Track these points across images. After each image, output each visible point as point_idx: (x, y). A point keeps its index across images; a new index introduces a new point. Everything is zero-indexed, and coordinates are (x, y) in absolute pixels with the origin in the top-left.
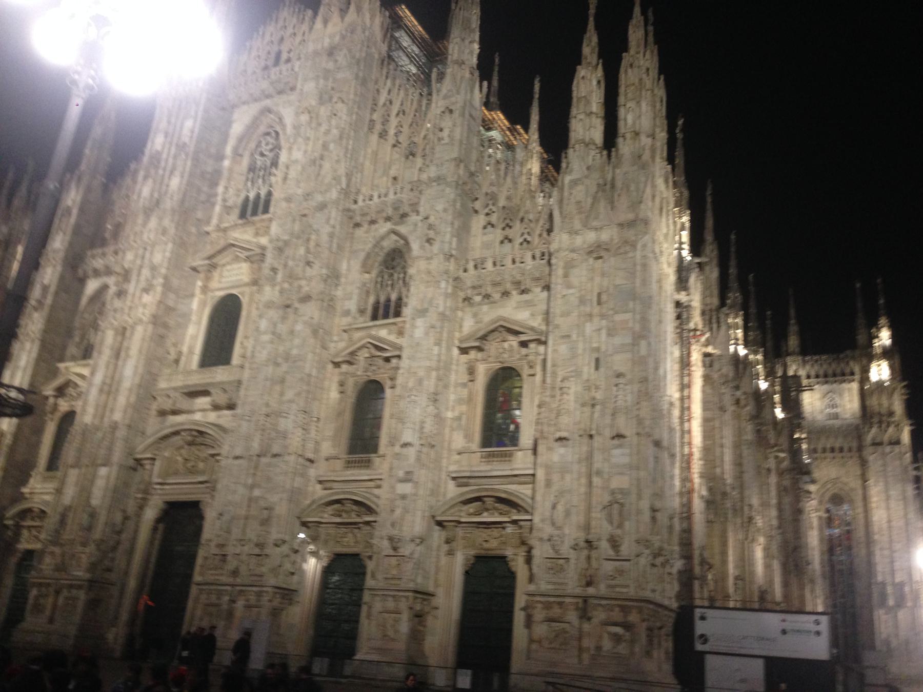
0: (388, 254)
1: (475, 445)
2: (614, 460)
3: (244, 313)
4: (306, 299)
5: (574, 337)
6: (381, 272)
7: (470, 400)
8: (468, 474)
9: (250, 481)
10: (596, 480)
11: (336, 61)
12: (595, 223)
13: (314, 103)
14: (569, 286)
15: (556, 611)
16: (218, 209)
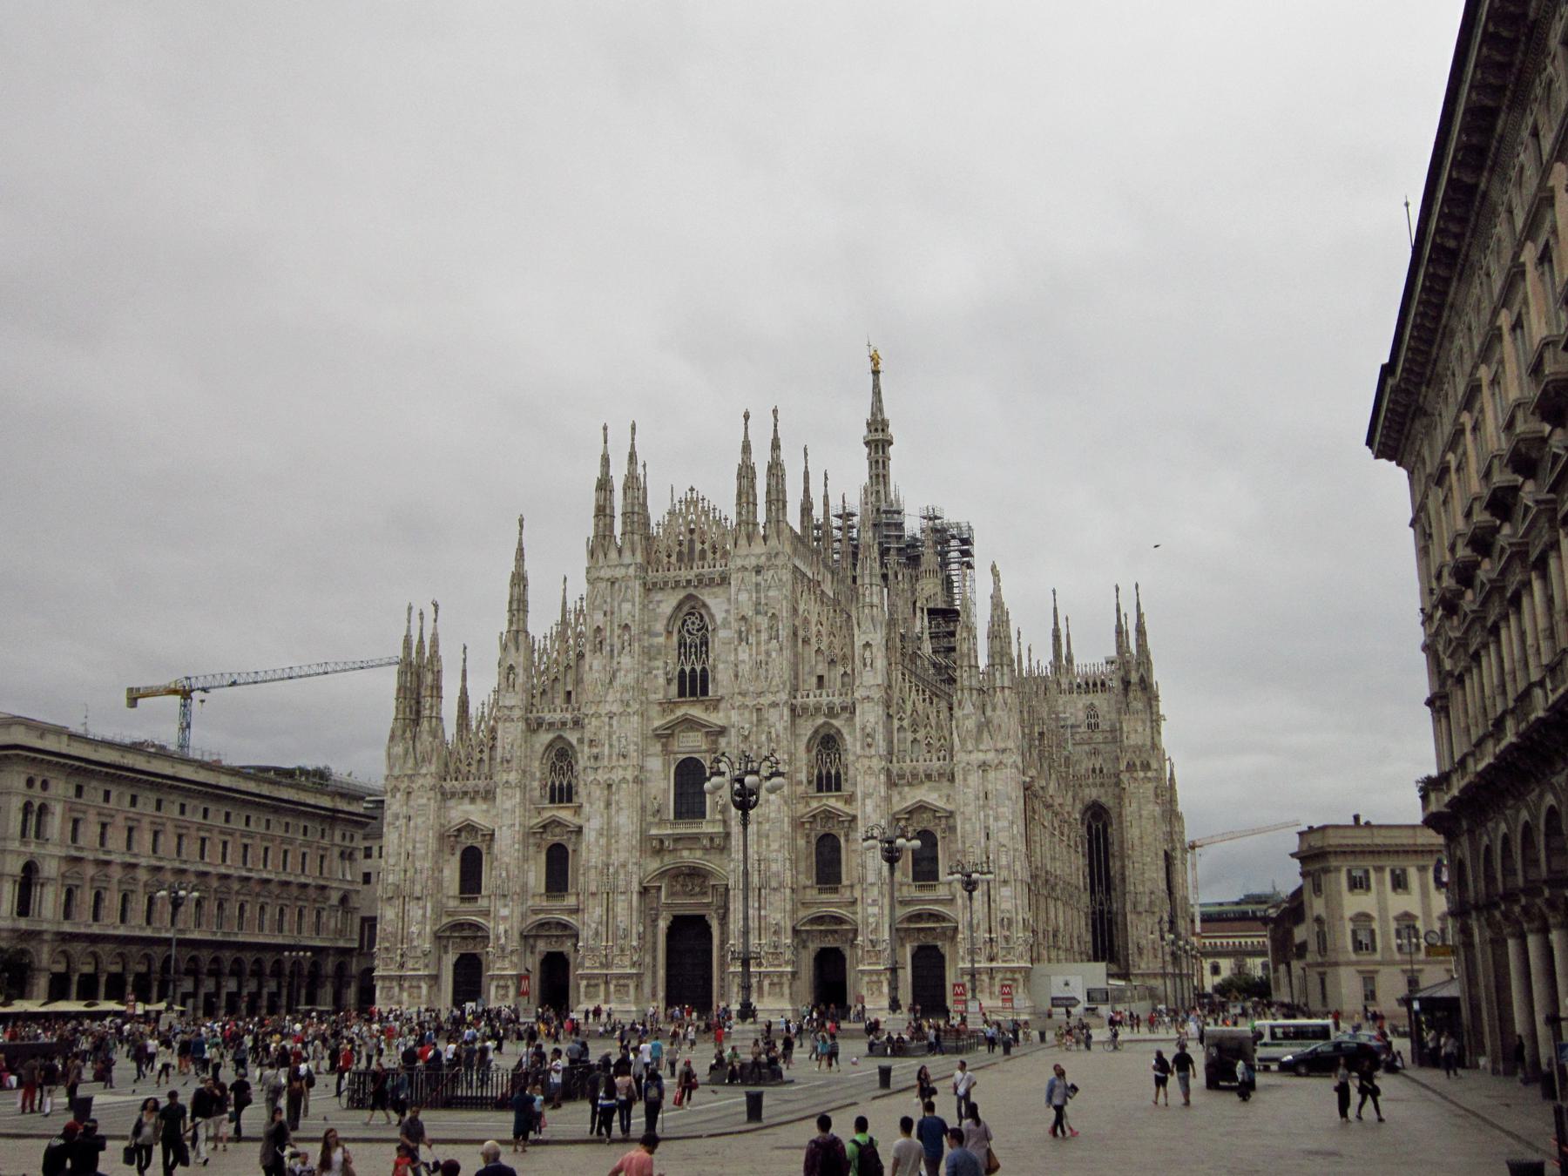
1: (910, 880)
16: (661, 681)
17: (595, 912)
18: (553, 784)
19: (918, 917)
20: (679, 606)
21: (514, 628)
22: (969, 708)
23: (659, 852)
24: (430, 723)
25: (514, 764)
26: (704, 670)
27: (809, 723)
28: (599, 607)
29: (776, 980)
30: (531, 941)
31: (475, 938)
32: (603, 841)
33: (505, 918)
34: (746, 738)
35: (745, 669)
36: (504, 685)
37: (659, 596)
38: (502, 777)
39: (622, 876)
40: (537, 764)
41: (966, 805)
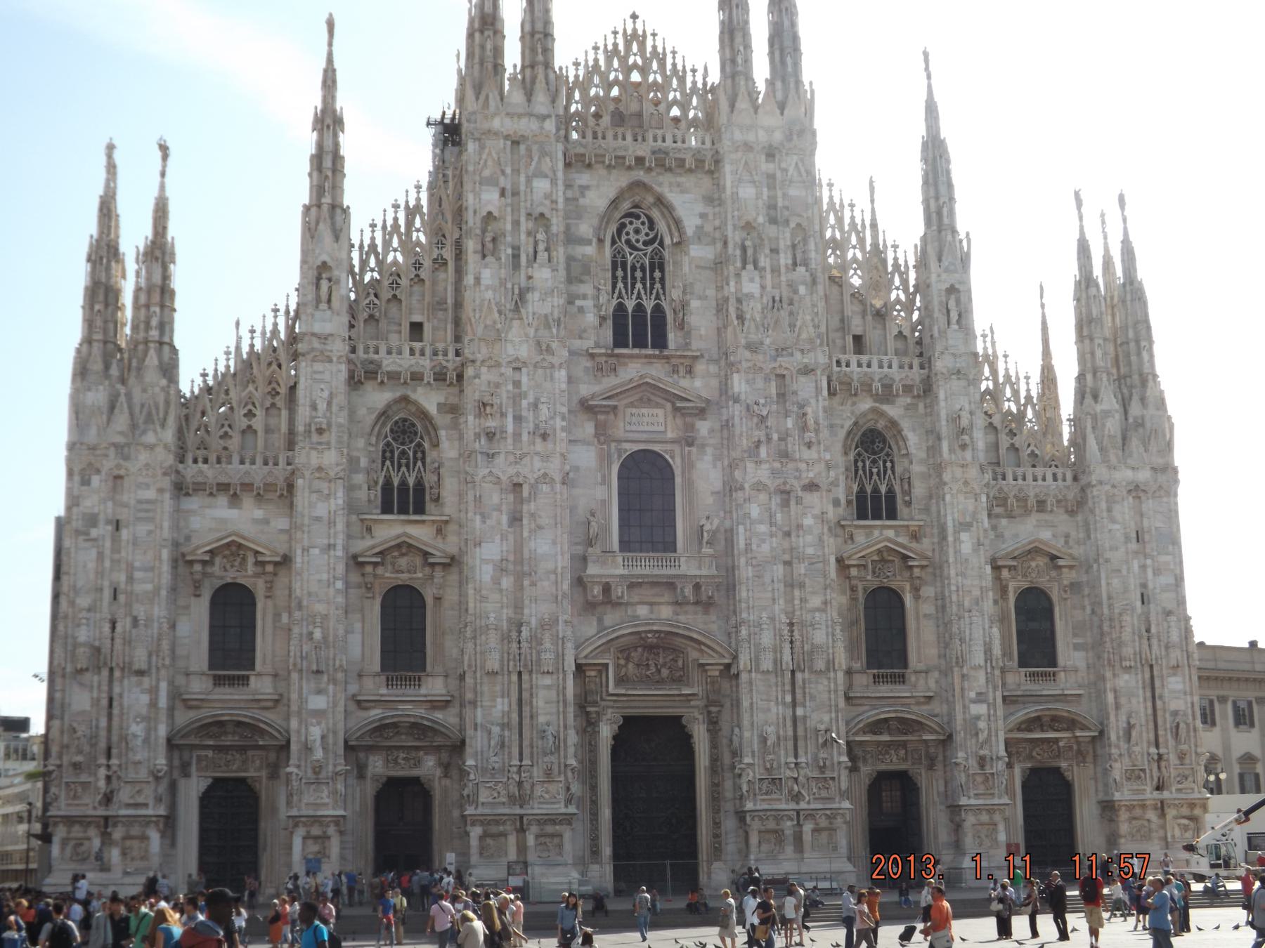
0: (864, 434)
2: (1170, 686)
3: (678, 480)
4: (812, 487)
5: (1124, 572)
6: (859, 454)
7: (1003, 619)
8: (1019, 693)
9: (789, 698)
10: (1159, 703)
11: (786, 170)
12: (1129, 461)
13: (761, 219)
14: (1113, 521)
15: (1138, 812)
16: (591, 318)
17: (495, 706)
18: (388, 484)
19: (1035, 723)
20: (615, 203)
21: (327, 200)
22: (1109, 401)
23: (590, 606)
24: (159, 352)
25: (332, 437)
26: (658, 309)
27: (848, 407)
28: (491, 181)
29: (824, 823)
30: (362, 755)
31: (243, 749)
32: (507, 582)
33: (319, 714)
34: (763, 419)
35: (754, 310)
36: (311, 296)
37: (584, 178)
38: (307, 457)
39: (547, 644)
40: (361, 443)
41: (1114, 548)
